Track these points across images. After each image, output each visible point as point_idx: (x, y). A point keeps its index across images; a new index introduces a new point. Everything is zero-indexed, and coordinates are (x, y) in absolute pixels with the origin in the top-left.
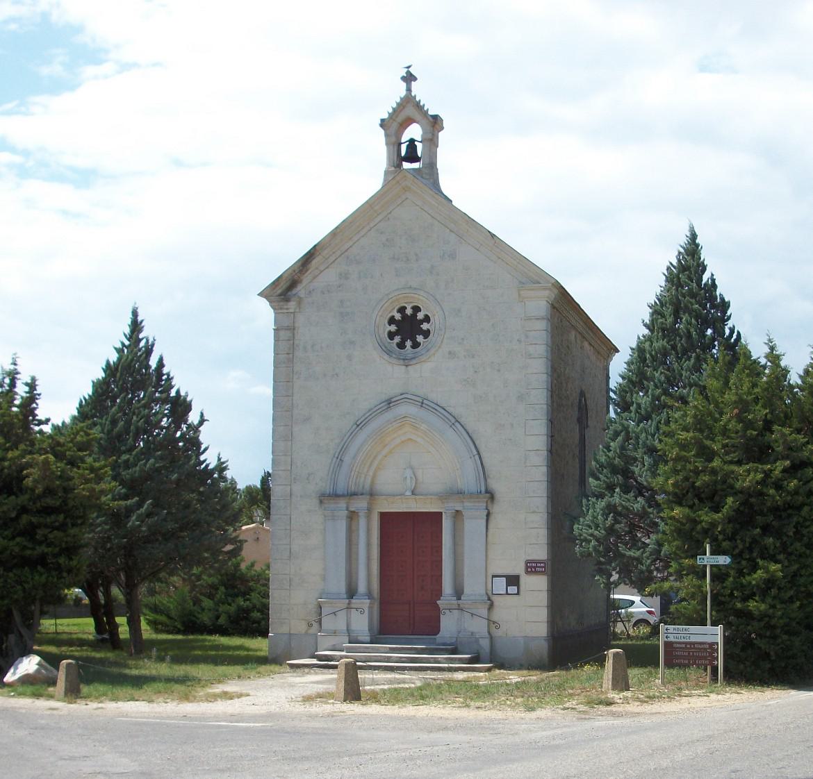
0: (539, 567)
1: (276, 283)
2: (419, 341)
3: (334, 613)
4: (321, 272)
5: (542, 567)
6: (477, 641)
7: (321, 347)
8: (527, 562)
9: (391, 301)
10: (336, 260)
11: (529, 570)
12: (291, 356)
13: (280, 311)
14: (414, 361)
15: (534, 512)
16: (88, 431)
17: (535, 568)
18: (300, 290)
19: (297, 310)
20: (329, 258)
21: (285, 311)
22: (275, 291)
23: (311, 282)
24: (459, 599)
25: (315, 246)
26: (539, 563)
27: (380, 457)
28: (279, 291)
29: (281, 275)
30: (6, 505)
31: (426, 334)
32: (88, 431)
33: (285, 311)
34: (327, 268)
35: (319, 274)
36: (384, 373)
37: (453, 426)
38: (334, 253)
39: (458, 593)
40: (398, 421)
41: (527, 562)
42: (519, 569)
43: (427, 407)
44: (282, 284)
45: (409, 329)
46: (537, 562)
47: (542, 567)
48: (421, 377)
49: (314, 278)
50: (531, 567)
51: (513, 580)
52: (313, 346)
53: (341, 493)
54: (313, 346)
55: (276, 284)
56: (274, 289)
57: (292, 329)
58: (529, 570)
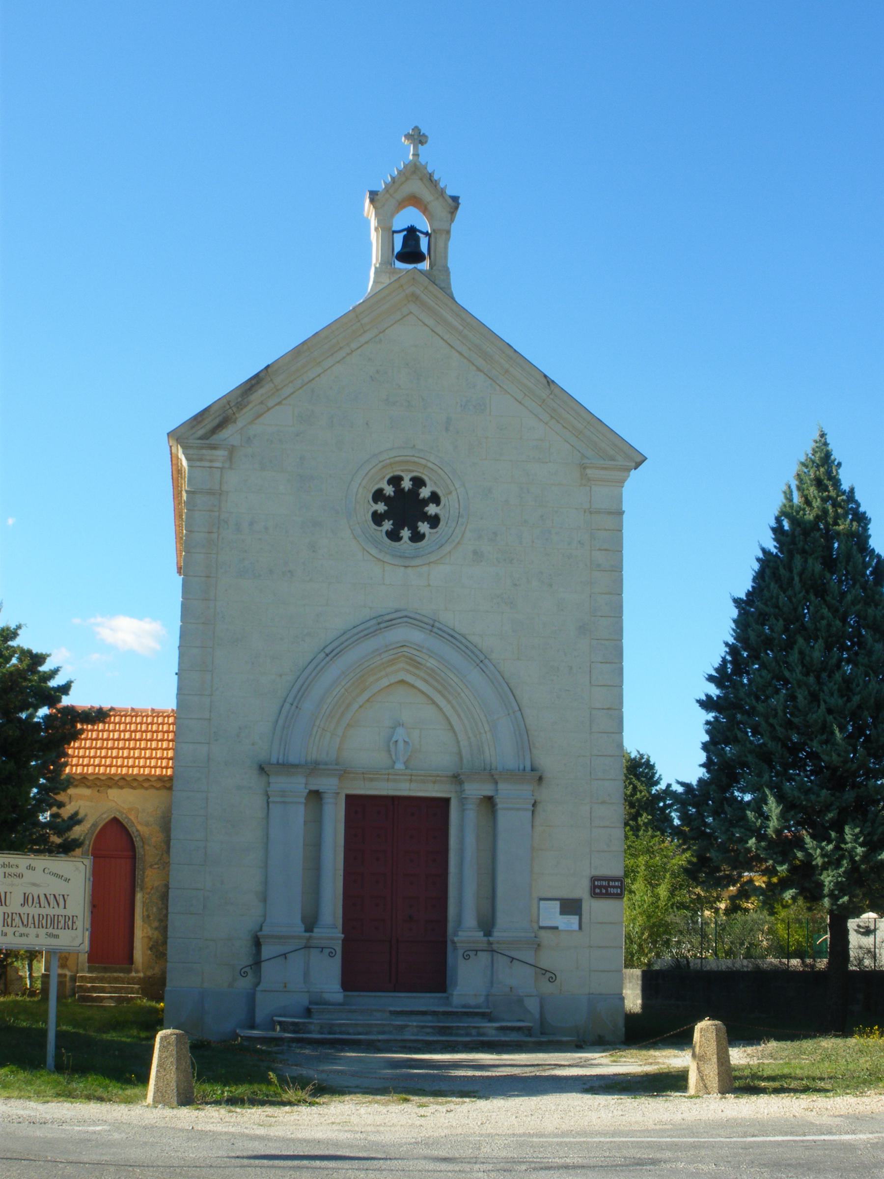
0: (614, 887)
1: (198, 418)
2: (422, 531)
3: (285, 955)
4: (269, 409)
5: (616, 887)
6: (520, 1001)
7: (266, 528)
8: (594, 879)
9: (380, 465)
10: (292, 394)
11: (598, 891)
12: (215, 536)
13: (198, 464)
14: (417, 562)
15: (603, 803)
16: (840, 853)
17: (606, 888)
18: (228, 434)
19: (227, 465)
20: (282, 388)
21: (207, 464)
22: (194, 431)
23: (251, 423)
24: (488, 933)
25: (268, 366)
26: (612, 880)
27: (356, 706)
28: (201, 432)
29: (210, 407)
30: (23, 904)
31: (434, 521)
32: (840, 853)
33: (207, 464)
34: (279, 403)
35: (265, 412)
36: (371, 576)
37: (481, 665)
38: (292, 382)
39: (487, 925)
40: (391, 652)
41: (594, 879)
42: (581, 890)
43: (440, 633)
44: (206, 422)
45: (405, 509)
46: (608, 879)
47: (616, 887)
48: (429, 585)
49: (259, 416)
50: (600, 887)
51: (571, 907)
52: (251, 524)
53: (296, 761)
54: (251, 524)
55: (200, 419)
56: (193, 427)
57: (217, 493)
58: (598, 891)
